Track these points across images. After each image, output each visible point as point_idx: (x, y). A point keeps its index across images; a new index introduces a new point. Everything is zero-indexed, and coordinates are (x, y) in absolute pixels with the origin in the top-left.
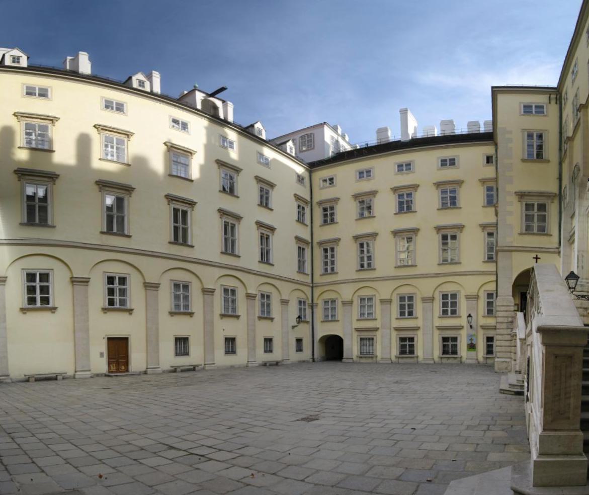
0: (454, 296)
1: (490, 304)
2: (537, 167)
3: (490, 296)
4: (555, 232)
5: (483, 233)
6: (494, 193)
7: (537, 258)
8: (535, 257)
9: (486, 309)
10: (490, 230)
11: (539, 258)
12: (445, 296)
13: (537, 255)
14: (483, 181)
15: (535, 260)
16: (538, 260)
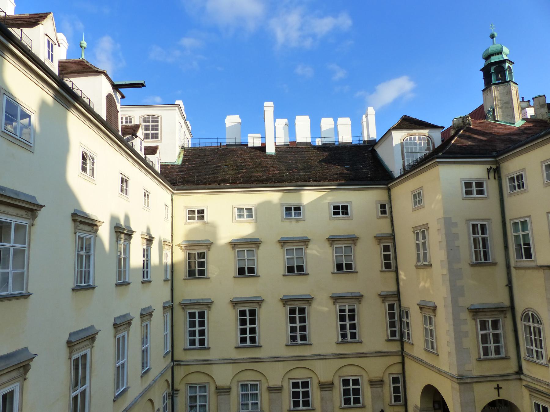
0: (356, 382)
1: (396, 390)
2: (484, 271)
3: (395, 380)
4: (512, 354)
5: (383, 305)
6: (391, 252)
7: (498, 388)
8: (496, 387)
9: (393, 395)
10: (391, 301)
11: (501, 388)
12: (346, 382)
13: (498, 385)
14: (379, 239)
15: (496, 391)
16: (500, 390)
